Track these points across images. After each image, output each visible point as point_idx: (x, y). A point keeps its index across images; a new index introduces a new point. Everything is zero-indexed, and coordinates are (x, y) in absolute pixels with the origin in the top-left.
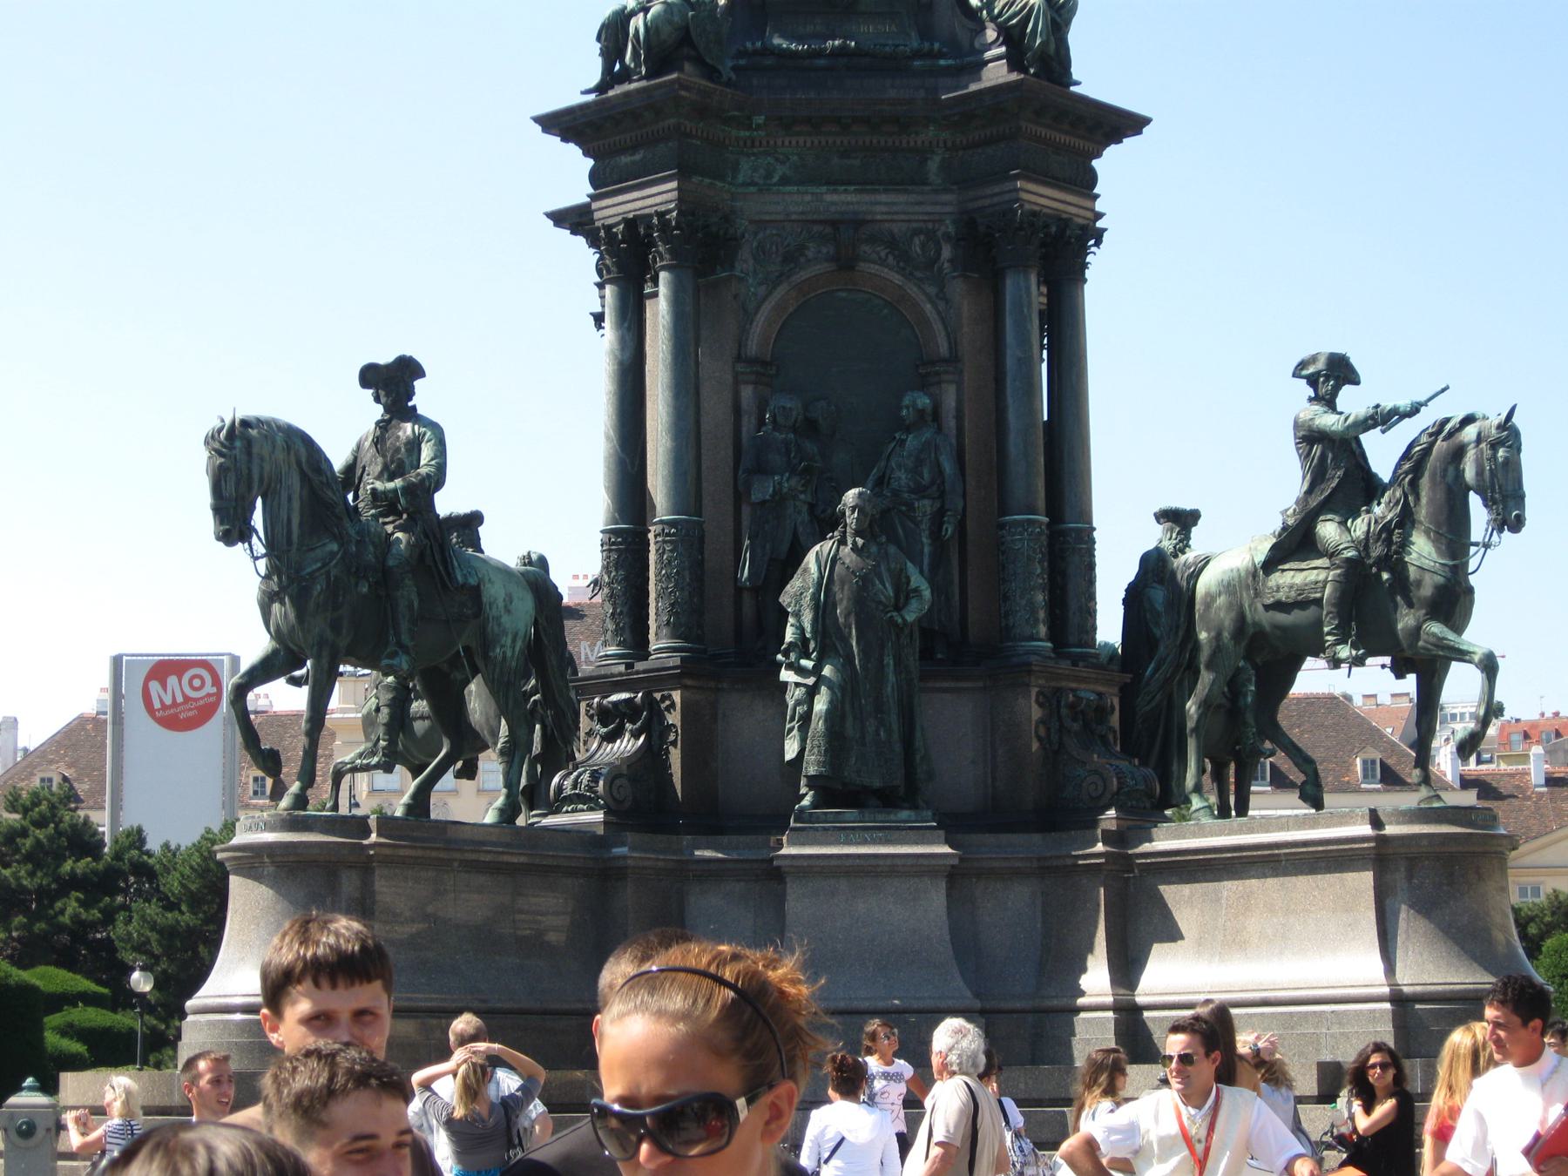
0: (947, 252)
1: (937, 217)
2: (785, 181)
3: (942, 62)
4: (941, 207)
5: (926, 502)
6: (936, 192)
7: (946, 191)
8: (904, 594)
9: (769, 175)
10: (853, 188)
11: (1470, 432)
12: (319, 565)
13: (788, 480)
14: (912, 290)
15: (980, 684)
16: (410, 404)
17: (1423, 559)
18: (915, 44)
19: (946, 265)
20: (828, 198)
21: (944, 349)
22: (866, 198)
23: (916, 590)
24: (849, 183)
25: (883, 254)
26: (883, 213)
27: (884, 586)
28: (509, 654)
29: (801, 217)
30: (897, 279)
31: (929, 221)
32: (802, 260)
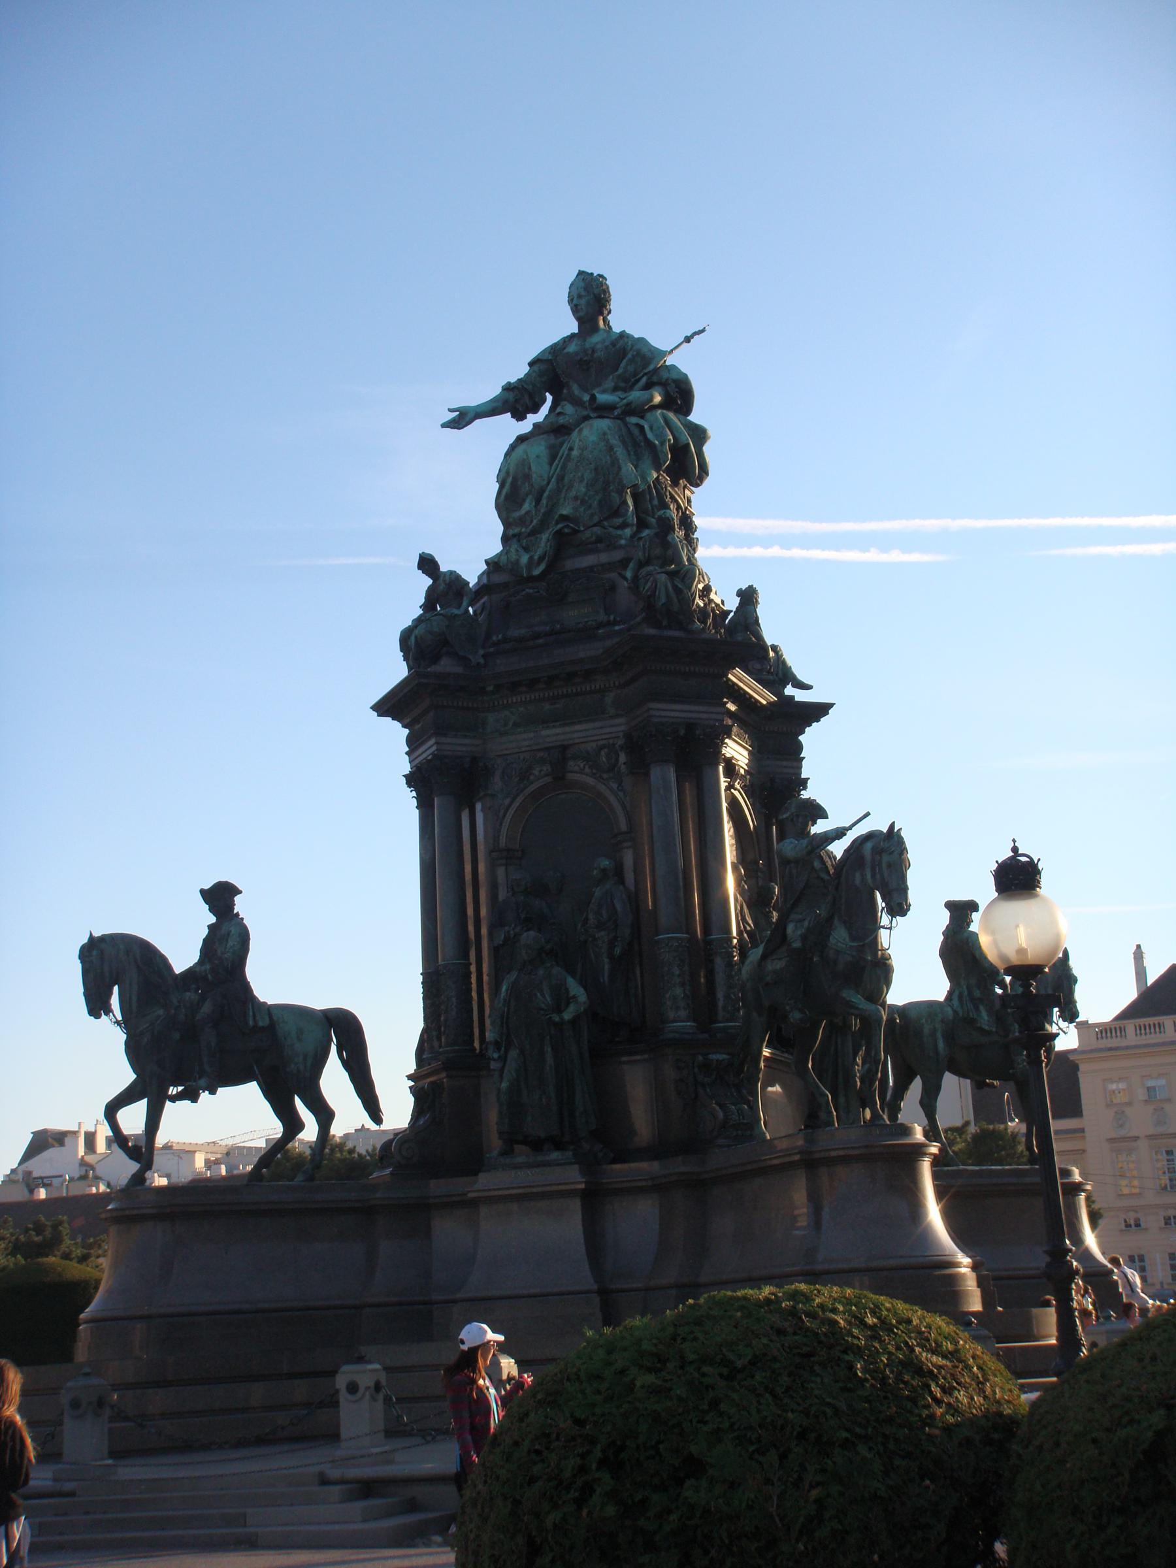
0: (623, 758)
1: (613, 735)
2: (516, 725)
3: (617, 628)
4: (615, 728)
5: (603, 933)
6: (611, 717)
7: (617, 716)
8: (562, 999)
9: (506, 725)
10: (558, 723)
11: (869, 846)
12: (148, 1025)
13: (513, 929)
14: (602, 788)
15: (646, 1056)
16: (235, 912)
17: (839, 944)
18: (602, 617)
19: (623, 767)
20: (545, 733)
21: (623, 826)
22: (567, 729)
23: (574, 997)
24: (556, 721)
25: (582, 766)
26: (579, 738)
27: (544, 997)
28: (302, 1068)
29: (529, 749)
30: (591, 781)
31: (610, 738)
32: (532, 777)
